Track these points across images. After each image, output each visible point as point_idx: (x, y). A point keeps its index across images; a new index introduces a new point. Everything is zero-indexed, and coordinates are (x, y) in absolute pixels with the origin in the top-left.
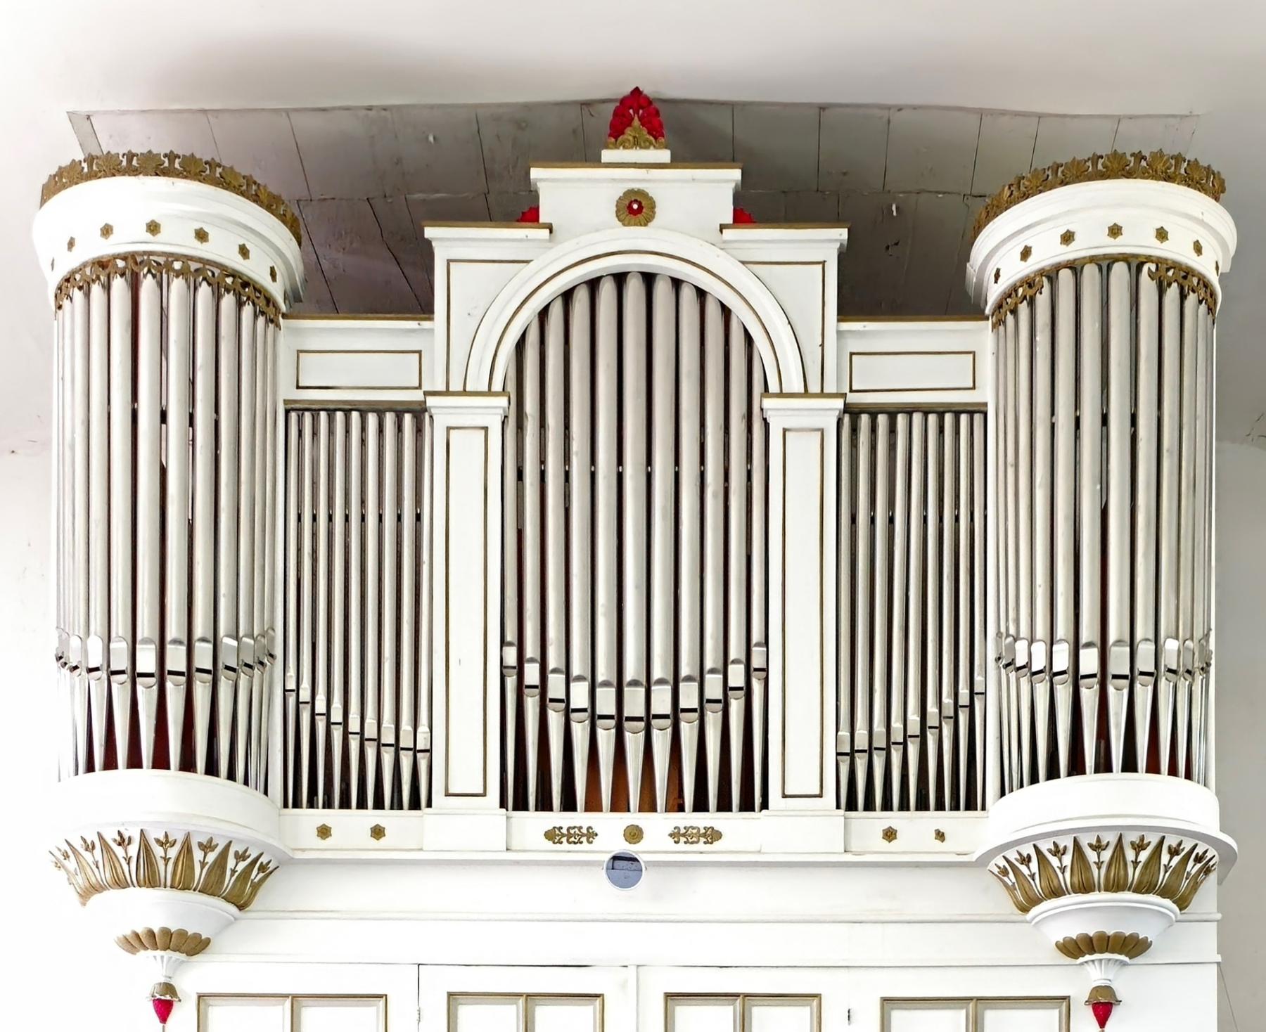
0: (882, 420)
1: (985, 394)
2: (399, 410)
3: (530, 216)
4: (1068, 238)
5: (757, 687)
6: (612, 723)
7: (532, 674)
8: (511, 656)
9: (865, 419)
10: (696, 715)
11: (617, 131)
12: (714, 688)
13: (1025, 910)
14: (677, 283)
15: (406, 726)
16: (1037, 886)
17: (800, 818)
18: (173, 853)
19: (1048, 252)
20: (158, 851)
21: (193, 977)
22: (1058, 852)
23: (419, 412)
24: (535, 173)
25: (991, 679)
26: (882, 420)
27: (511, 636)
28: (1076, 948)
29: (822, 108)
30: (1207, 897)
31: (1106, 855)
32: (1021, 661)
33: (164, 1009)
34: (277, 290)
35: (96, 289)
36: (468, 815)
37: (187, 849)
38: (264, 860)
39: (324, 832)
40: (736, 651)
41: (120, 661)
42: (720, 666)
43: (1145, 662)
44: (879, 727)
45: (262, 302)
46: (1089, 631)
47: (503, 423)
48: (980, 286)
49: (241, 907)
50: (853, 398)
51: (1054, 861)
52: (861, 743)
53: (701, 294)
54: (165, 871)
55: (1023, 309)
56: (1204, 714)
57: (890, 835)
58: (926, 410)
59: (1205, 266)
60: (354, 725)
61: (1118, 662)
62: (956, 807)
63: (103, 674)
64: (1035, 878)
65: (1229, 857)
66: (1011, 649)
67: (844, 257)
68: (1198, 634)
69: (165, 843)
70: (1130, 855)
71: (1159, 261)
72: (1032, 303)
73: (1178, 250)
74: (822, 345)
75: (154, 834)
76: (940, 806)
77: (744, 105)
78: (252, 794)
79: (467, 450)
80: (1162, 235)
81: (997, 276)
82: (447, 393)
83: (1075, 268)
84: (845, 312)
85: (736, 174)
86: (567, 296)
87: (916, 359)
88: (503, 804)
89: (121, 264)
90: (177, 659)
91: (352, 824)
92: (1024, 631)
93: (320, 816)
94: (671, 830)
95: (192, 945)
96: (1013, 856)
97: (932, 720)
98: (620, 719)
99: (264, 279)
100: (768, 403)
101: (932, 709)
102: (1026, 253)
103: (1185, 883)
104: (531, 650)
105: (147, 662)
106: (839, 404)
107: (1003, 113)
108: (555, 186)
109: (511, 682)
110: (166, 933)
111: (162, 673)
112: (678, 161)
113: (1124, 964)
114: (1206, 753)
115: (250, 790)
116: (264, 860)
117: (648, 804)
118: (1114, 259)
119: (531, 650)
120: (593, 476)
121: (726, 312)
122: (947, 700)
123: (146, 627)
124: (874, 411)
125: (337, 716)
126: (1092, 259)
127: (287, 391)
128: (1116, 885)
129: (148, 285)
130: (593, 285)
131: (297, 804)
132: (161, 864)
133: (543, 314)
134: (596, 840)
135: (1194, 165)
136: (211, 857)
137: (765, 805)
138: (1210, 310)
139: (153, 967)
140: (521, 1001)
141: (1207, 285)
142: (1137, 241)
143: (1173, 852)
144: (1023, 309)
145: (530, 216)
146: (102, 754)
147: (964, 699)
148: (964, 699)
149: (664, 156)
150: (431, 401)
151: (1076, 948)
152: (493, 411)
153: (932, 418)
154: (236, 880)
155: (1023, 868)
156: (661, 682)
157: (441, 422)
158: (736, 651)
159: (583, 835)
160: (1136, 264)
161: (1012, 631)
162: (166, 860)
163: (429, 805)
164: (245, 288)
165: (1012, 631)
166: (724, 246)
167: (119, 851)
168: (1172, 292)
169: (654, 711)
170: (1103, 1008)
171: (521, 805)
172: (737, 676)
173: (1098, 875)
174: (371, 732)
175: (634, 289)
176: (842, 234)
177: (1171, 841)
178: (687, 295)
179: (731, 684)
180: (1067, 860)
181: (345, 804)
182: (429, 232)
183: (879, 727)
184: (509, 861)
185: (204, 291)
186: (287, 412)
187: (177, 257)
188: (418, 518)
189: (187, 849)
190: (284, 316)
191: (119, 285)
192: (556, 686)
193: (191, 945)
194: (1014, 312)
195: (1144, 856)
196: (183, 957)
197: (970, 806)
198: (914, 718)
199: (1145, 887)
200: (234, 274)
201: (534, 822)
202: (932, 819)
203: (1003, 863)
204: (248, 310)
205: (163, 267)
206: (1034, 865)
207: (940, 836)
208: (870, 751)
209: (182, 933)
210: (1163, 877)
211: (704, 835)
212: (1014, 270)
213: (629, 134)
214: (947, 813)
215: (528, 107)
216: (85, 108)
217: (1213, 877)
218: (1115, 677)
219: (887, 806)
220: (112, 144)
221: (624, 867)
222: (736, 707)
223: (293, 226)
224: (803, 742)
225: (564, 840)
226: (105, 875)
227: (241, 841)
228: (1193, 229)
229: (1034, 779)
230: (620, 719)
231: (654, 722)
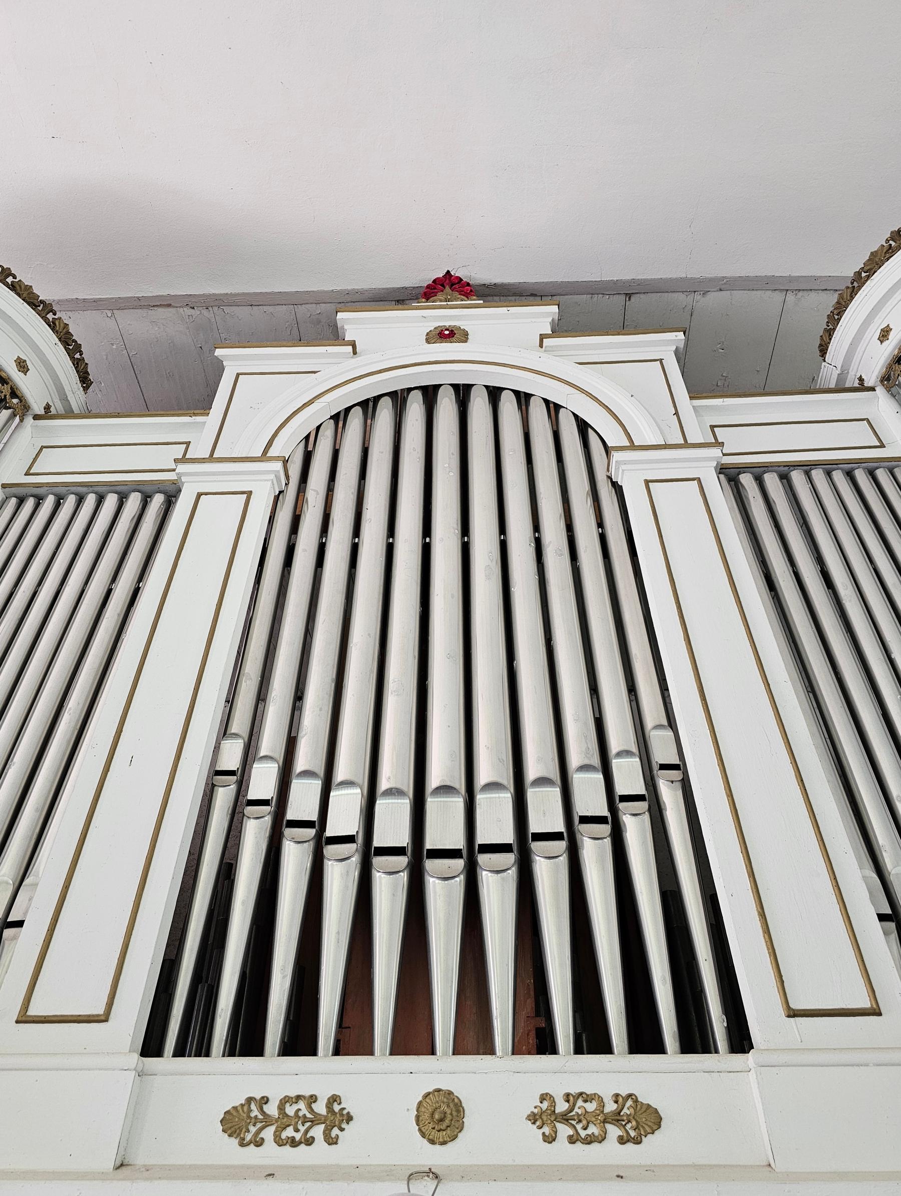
5: (670, 796)
6: (402, 861)
7: (263, 782)
8: (231, 758)
10: (561, 846)
27: (240, 723)
47: (277, 499)
74: (676, 413)
85: (555, 309)
94: (532, 1104)
98: (418, 854)
109: (224, 796)
117: (474, 1036)
120: (390, 550)
124: (759, 473)
134: (349, 1135)
137: (740, 1041)
152: (264, 483)
159: (316, 1120)
169: (481, 838)
172: (628, 777)
175: (446, 407)
179: (621, 789)
211: (616, 1118)
225: (268, 1134)
230: (418, 854)
231: (483, 859)
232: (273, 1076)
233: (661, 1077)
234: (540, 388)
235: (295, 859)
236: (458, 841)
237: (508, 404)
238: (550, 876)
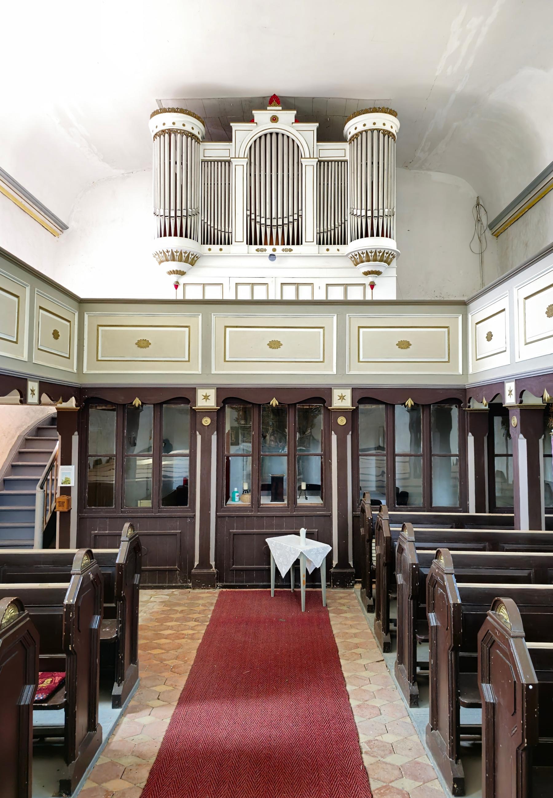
0: (326, 163)
1: (347, 158)
2: (225, 161)
3: (252, 121)
4: (364, 125)
8: (249, 213)
9: (322, 163)
11: (271, 103)
12: (291, 219)
13: (356, 265)
14: (283, 135)
15: (227, 227)
16: (358, 260)
17: (309, 246)
18: (178, 254)
19: (360, 128)
20: (175, 254)
21: (182, 280)
22: (363, 253)
23: (229, 162)
24: (253, 112)
25: (349, 217)
26: (326, 163)
27: (249, 208)
28: (366, 273)
29: (313, 98)
30: (394, 263)
31: (373, 254)
32: (355, 214)
33: (176, 287)
34: (200, 137)
35: (162, 136)
36: (240, 246)
37: (181, 253)
39: (210, 250)
40: (295, 211)
41: (167, 214)
43: (381, 214)
44: (325, 227)
46: (369, 207)
48: (346, 135)
50: (320, 159)
51: (362, 255)
52: (322, 231)
53: (288, 137)
54: (177, 258)
55: (355, 140)
56: (393, 224)
57: (328, 250)
58: (335, 161)
59: (393, 131)
60: (216, 227)
61: (375, 214)
62: (341, 244)
64: (358, 259)
65: (398, 254)
66: (353, 211)
67: (318, 129)
68: (392, 208)
69: (177, 252)
70: (378, 254)
71: (384, 130)
75: (174, 250)
76: (338, 244)
79: (239, 170)
80: (384, 124)
82: (235, 158)
83: (366, 131)
84: (319, 140)
85: (295, 112)
86: (260, 138)
87: (333, 150)
88: (247, 244)
90: (179, 214)
92: (356, 207)
93: (209, 246)
95: (182, 273)
96: (353, 254)
97: (337, 226)
98: (271, 226)
99: (197, 134)
100: (302, 160)
101: (336, 224)
102: (356, 128)
104: (253, 211)
105: (173, 214)
106: (317, 160)
107: (351, 99)
108: (258, 115)
109: (249, 218)
110: (177, 271)
111: (176, 216)
114: (394, 233)
115: (194, 241)
117: (277, 244)
118: (374, 129)
119: (253, 211)
120: (266, 175)
121: (293, 141)
122: (340, 222)
124: (324, 162)
125: (212, 225)
126: (370, 130)
127: (202, 158)
128: (375, 260)
129: (173, 135)
131: (204, 244)
133: (255, 141)
135: (391, 110)
136: (186, 255)
137: (302, 244)
138: (394, 140)
139: (174, 278)
141: (393, 135)
142: (379, 126)
143: (387, 253)
144: (355, 140)
145: (252, 121)
146: (163, 234)
147: (343, 222)
148: (343, 222)
149: (280, 108)
150: (232, 160)
151: (366, 273)
152: (245, 162)
153: (336, 163)
154: (192, 260)
156: (280, 218)
157: (234, 164)
158: (295, 211)
160: (379, 130)
164: (193, 136)
167: (167, 254)
168: (386, 136)
170: (372, 286)
171: (251, 244)
172: (296, 217)
173: (371, 258)
174: (219, 229)
175: (274, 136)
176: (317, 124)
177: (386, 251)
178: (285, 137)
180: (365, 255)
181: (214, 244)
182: (231, 124)
183: (325, 227)
184: (248, 256)
185: (184, 137)
187: (179, 130)
188: (229, 184)
189: (181, 253)
191: (167, 135)
192: (258, 219)
193: (182, 273)
194: (353, 141)
195: (381, 254)
197: (345, 244)
198: (333, 225)
199: (381, 261)
201: (254, 248)
202: (337, 247)
204: (193, 141)
205: (176, 132)
206: (358, 256)
207: (338, 250)
208: (324, 232)
209: (180, 271)
210: (385, 259)
212: (353, 132)
214: (340, 245)
215: (252, 98)
216: (159, 98)
217: (395, 258)
219: (327, 244)
220: (165, 106)
221: (272, 257)
222: (296, 223)
224: (310, 230)
228: (391, 123)
229: (358, 238)
230: (271, 226)
234: (291, 136)
236: (276, 224)
237: (285, 137)
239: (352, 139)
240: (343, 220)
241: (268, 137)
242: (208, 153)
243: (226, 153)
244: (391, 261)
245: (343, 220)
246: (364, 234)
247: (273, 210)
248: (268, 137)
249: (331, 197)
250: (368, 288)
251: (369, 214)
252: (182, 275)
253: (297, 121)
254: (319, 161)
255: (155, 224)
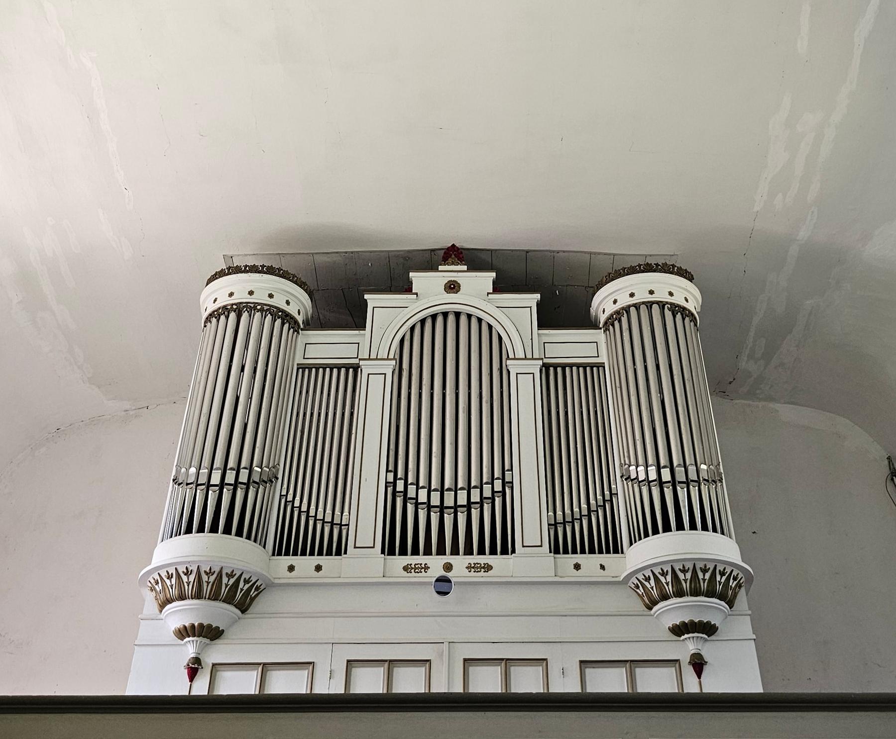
0: (559, 370)
1: (603, 359)
3: (408, 289)
4: (632, 295)
5: (508, 491)
12: (487, 493)
13: (650, 609)
14: (469, 316)
15: (338, 512)
16: (655, 593)
17: (532, 559)
19: (624, 301)
20: (205, 578)
22: (664, 574)
23: (356, 368)
24: (411, 274)
25: (619, 486)
26: (559, 370)
28: (679, 630)
29: (527, 252)
30: (742, 599)
32: (633, 476)
34: (300, 319)
36: (364, 560)
38: (258, 583)
41: (203, 479)
42: (490, 481)
45: (292, 323)
46: (663, 461)
48: (596, 316)
49: (243, 612)
50: (546, 361)
52: (560, 518)
53: (480, 320)
54: (206, 589)
55: (616, 323)
58: (578, 366)
59: (691, 306)
60: (312, 513)
61: (680, 476)
62: (608, 552)
63: (193, 486)
65: (750, 578)
66: (628, 471)
68: (715, 463)
69: (209, 573)
71: (671, 304)
72: (620, 321)
73: (678, 300)
75: (205, 568)
76: (601, 552)
77: (496, 250)
78: (257, 547)
79: (376, 383)
81: (604, 311)
82: (369, 359)
83: (637, 306)
84: (540, 326)
85: (494, 274)
86: (423, 322)
88: (383, 552)
89: (235, 307)
90: (230, 478)
91: (305, 564)
94: (467, 565)
96: (641, 577)
97: (593, 508)
99: (295, 314)
100: (509, 362)
101: (592, 502)
102: (615, 302)
103: (730, 592)
105: (216, 479)
106: (540, 362)
107: (599, 254)
108: (418, 279)
109: (390, 490)
110: (201, 625)
111: (222, 484)
112: (469, 270)
113: (706, 640)
115: (257, 545)
116: (258, 583)
117: (455, 551)
121: (490, 327)
123: (218, 462)
124: (555, 366)
125: (304, 508)
126: (643, 303)
127: (299, 360)
128: (696, 592)
129: (245, 316)
130: (434, 317)
131: (279, 554)
132: (205, 584)
133: (412, 329)
135: (680, 269)
137: (513, 551)
138: (696, 325)
139: (190, 648)
140: (386, 664)
141: (692, 314)
143: (722, 574)
144: (616, 323)
145: (408, 289)
146: (189, 525)
147: (607, 497)
148: (607, 497)
149: (465, 268)
150: (362, 363)
151: (679, 630)
152: (389, 367)
153: (581, 369)
155: (647, 584)
156: (462, 489)
157: (365, 372)
160: (662, 305)
161: (627, 462)
162: (208, 583)
163: (345, 553)
164: (286, 317)
165: (627, 462)
166: (489, 301)
171: (392, 552)
172: (498, 486)
173: (686, 586)
174: (320, 516)
175: (451, 319)
177: (720, 568)
178: (474, 321)
181: (304, 553)
182: (366, 297)
186: (298, 369)
187: (259, 304)
188: (352, 414)
190: (302, 330)
191: (233, 316)
193: (210, 633)
194: (613, 325)
196: (207, 641)
198: (584, 506)
199: (711, 593)
200: (283, 311)
201: (400, 561)
203: (636, 581)
204: (286, 326)
205: (251, 308)
206: (652, 582)
207: (602, 567)
208: (564, 523)
211: (484, 568)
212: (611, 309)
213: (450, 260)
214: (604, 555)
215: (409, 251)
216: (230, 253)
217: (743, 589)
218: (680, 482)
219: (574, 552)
221: (443, 586)
222: (498, 501)
223: (311, 294)
226: (175, 592)
227: (248, 572)
229: (647, 535)
232: (410, 560)
233: (496, 561)
235: (410, 508)
236: (452, 504)
237: (474, 321)
238: (475, 513)
239: (610, 322)
240: (607, 493)
241: (440, 319)
242: (312, 352)
243: (351, 351)
244: (735, 595)
245: (607, 493)
246: (660, 523)
247: (447, 470)
248: (440, 319)
249: (572, 440)
250: (689, 673)
251: (666, 475)
252: (213, 638)
253: (498, 288)
254: (544, 365)
255: (170, 502)
